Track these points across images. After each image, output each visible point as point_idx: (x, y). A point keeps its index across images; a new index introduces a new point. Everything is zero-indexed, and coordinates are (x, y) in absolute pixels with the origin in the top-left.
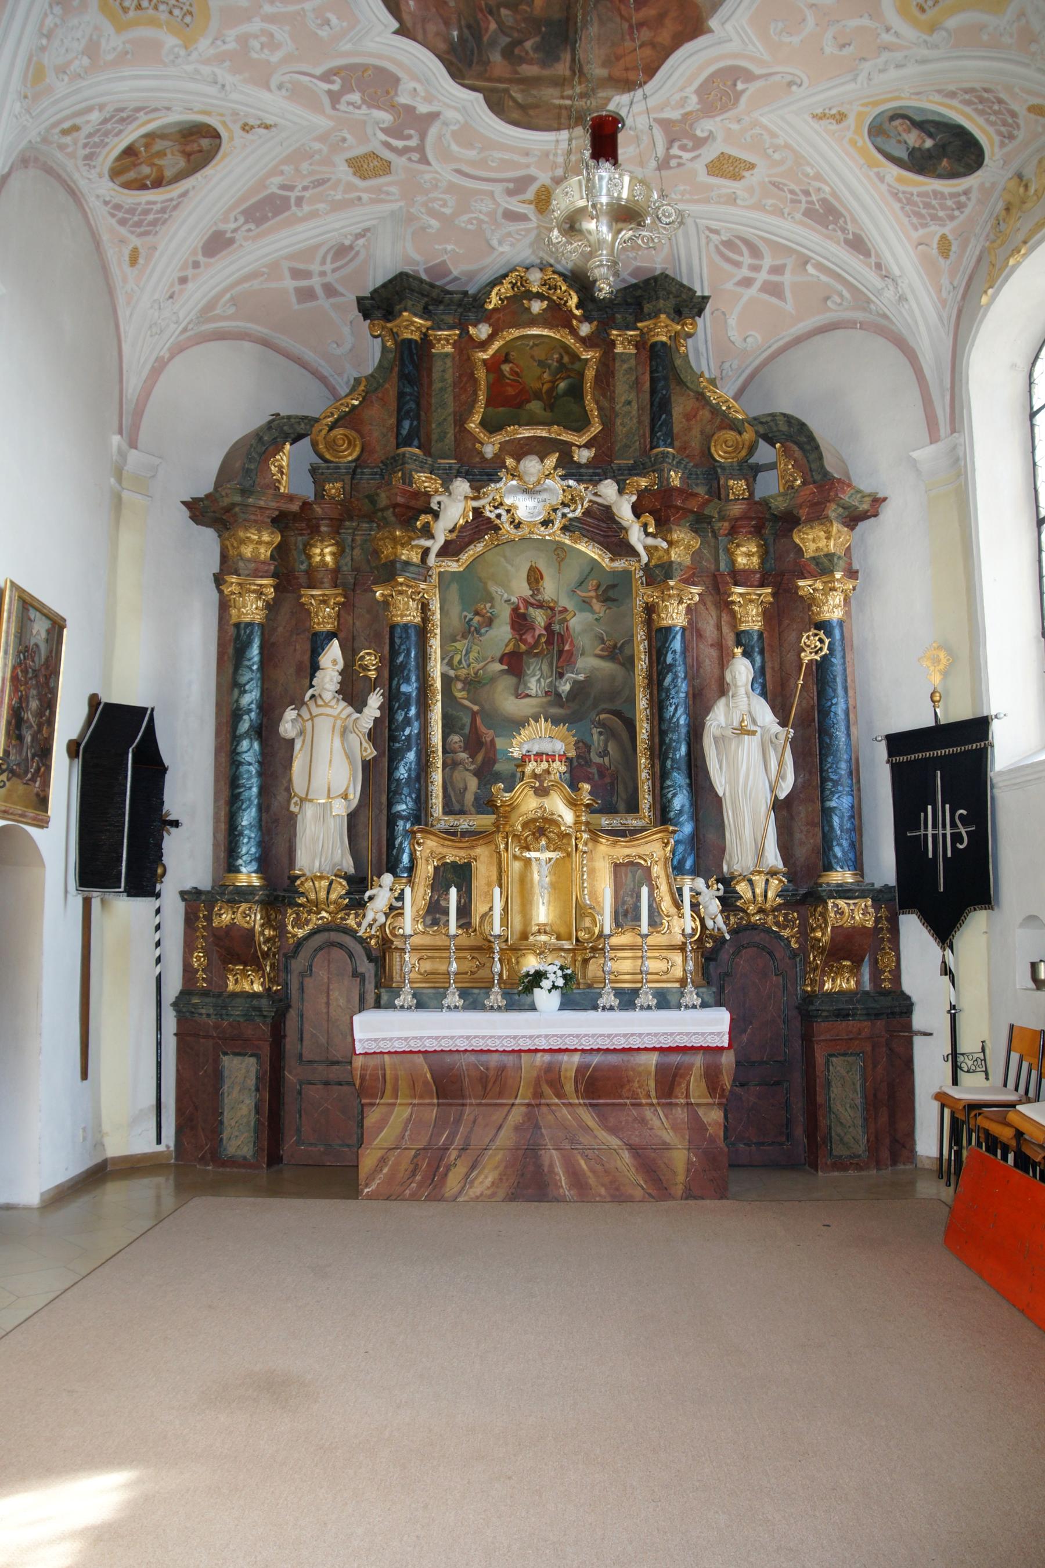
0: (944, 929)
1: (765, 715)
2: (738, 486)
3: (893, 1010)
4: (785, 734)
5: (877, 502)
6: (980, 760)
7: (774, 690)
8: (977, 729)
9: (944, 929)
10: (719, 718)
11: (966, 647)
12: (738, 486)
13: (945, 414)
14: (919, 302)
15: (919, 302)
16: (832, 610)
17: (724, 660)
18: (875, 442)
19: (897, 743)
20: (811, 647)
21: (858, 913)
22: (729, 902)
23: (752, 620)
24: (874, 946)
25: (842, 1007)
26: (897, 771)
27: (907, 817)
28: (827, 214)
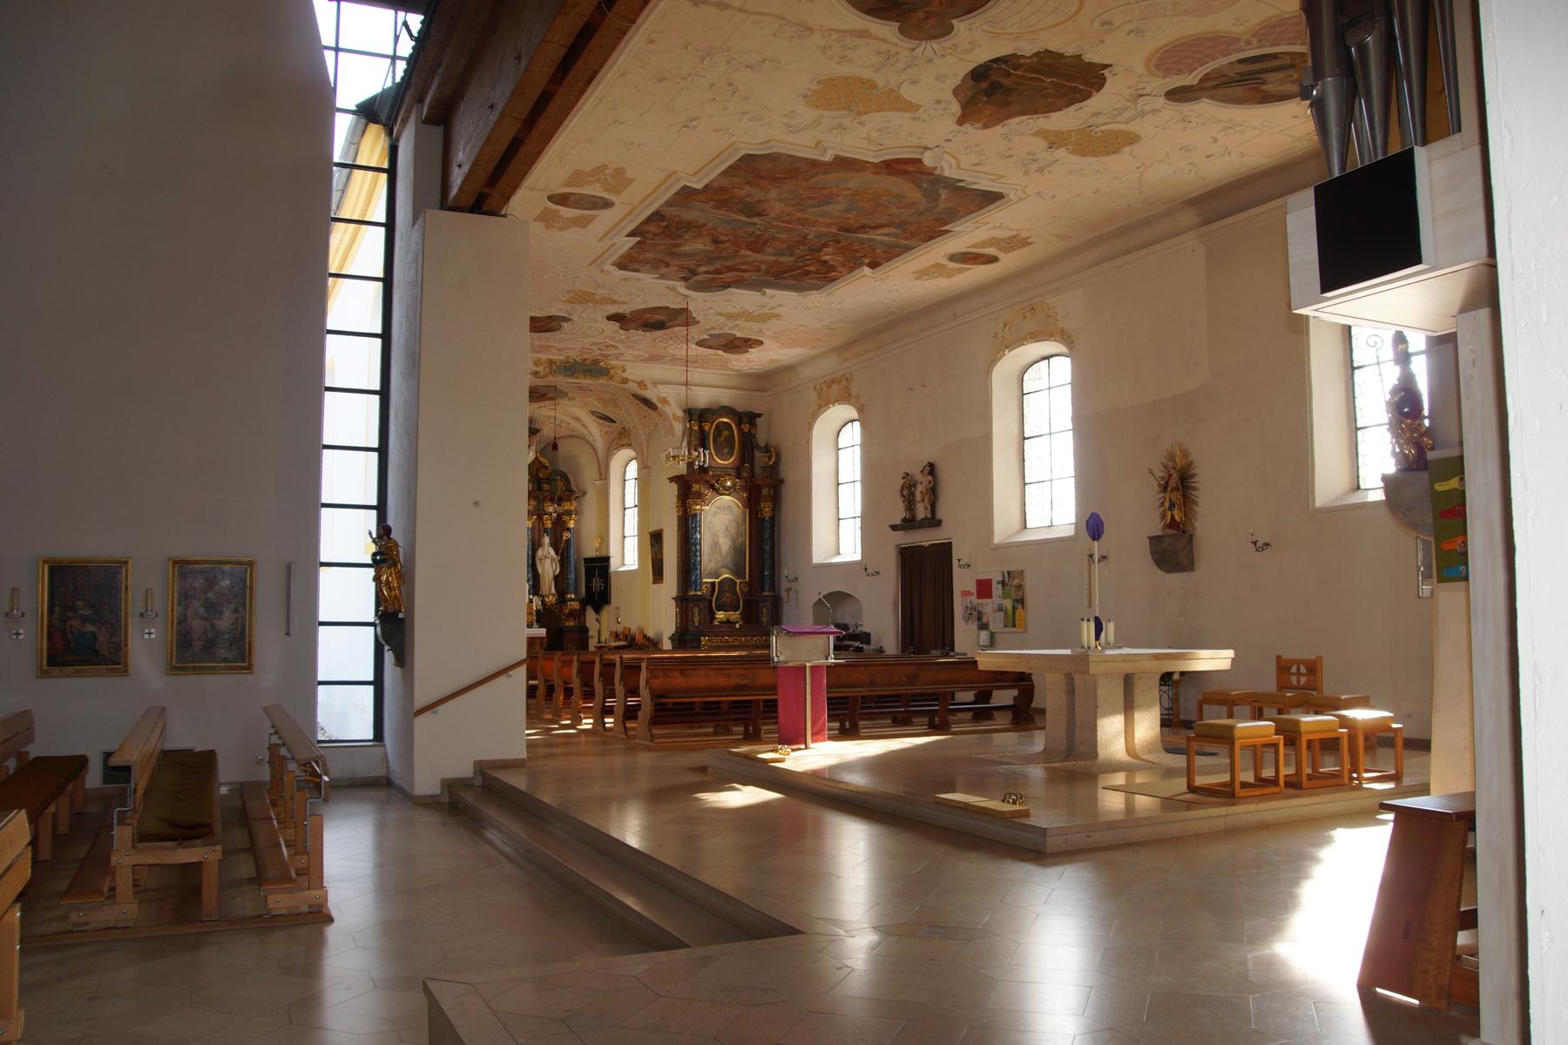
0: (598, 610)
1: (552, 553)
2: (546, 487)
3: (584, 631)
4: (557, 558)
5: (584, 494)
6: (607, 567)
7: (555, 545)
8: (607, 559)
9: (598, 610)
10: (540, 553)
11: (604, 537)
12: (546, 487)
13: (604, 475)
14: (600, 444)
15: (600, 444)
16: (571, 525)
17: (541, 537)
18: (587, 476)
19: (587, 560)
20: (566, 535)
21: (575, 605)
22: (543, 603)
23: (549, 524)
24: (579, 615)
25: (571, 630)
26: (587, 568)
27: (588, 581)
28: (577, 419)
